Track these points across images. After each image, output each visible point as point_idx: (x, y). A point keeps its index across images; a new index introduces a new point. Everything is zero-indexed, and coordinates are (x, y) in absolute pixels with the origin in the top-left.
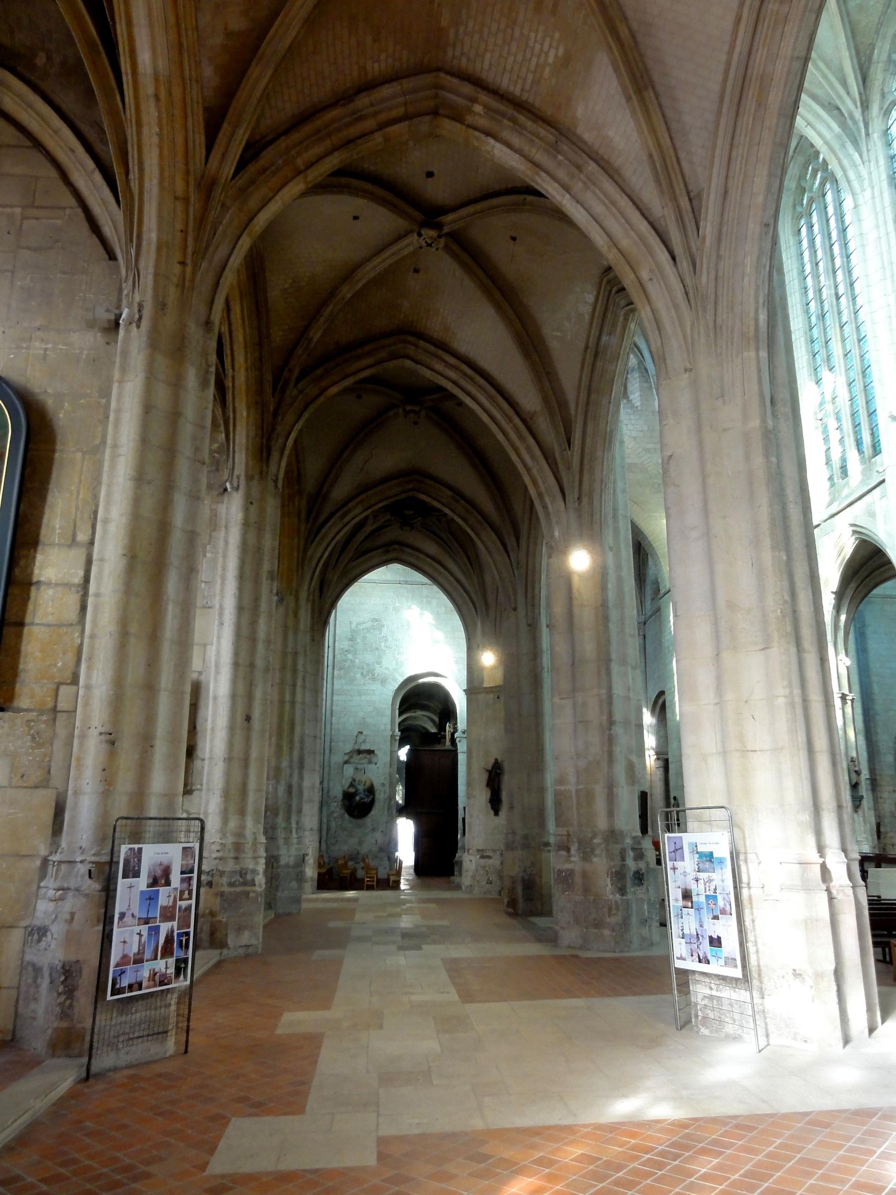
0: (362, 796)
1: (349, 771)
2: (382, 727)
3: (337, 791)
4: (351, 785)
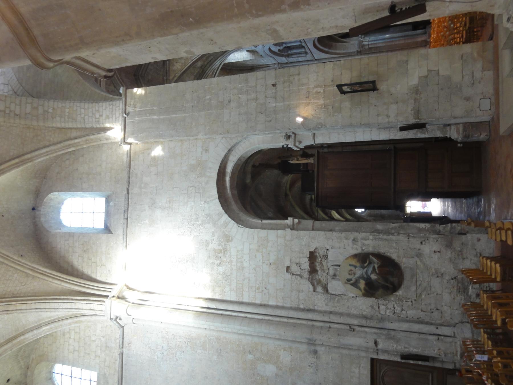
0: (371, 269)
1: (336, 286)
2: (281, 241)
3: (365, 305)
4: (355, 284)
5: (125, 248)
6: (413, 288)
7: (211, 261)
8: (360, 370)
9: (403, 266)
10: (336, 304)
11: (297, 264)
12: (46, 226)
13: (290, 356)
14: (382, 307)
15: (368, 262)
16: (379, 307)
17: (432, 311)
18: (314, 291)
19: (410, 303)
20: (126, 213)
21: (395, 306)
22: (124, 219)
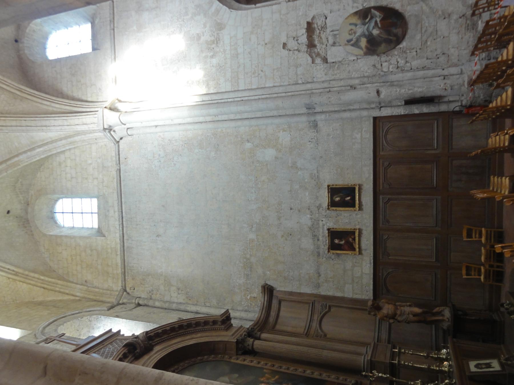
0: (373, 24)
3: (366, 64)
4: (356, 44)
5: (113, 61)
6: (418, 37)
7: (204, 55)
8: (362, 134)
9: (407, 15)
10: (336, 72)
11: (294, 38)
12: (31, 58)
13: (289, 135)
14: (385, 64)
15: (369, 17)
16: (381, 65)
17: (438, 56)
18: (313, 62)
19: (415, 53)
20: (112, 23)
21: (399, 60)
22: (110, 30)
